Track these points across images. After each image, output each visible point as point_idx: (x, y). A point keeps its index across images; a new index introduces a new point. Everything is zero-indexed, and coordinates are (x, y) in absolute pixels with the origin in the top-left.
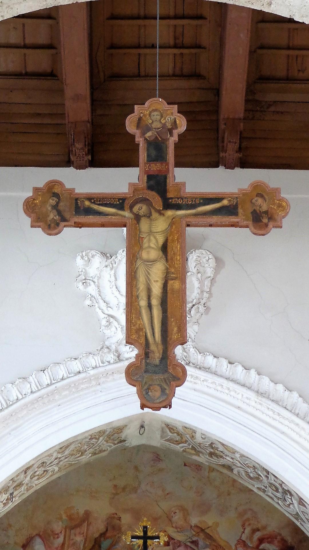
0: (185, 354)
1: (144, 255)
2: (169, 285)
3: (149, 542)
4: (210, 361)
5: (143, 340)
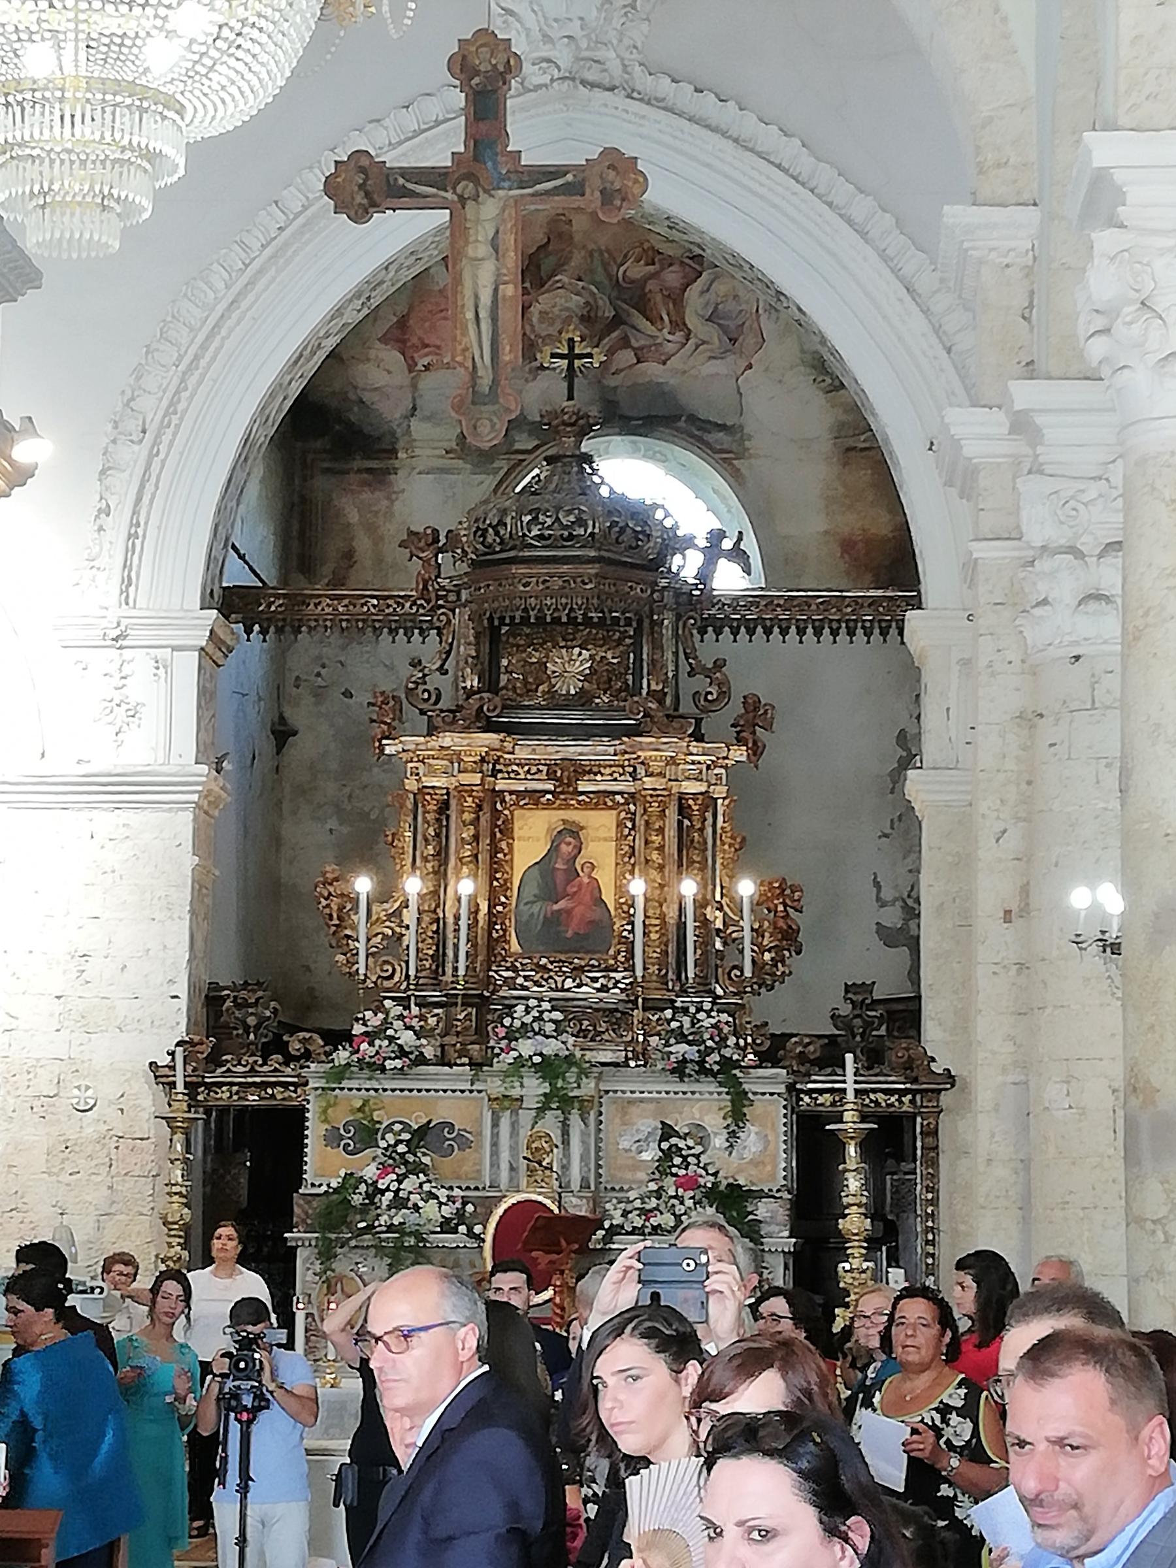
0: (626, 76)
1: (471, 251)
2: (500, 292)
3: (577, 363)
4: (665, 86)
5: (469, 364)
